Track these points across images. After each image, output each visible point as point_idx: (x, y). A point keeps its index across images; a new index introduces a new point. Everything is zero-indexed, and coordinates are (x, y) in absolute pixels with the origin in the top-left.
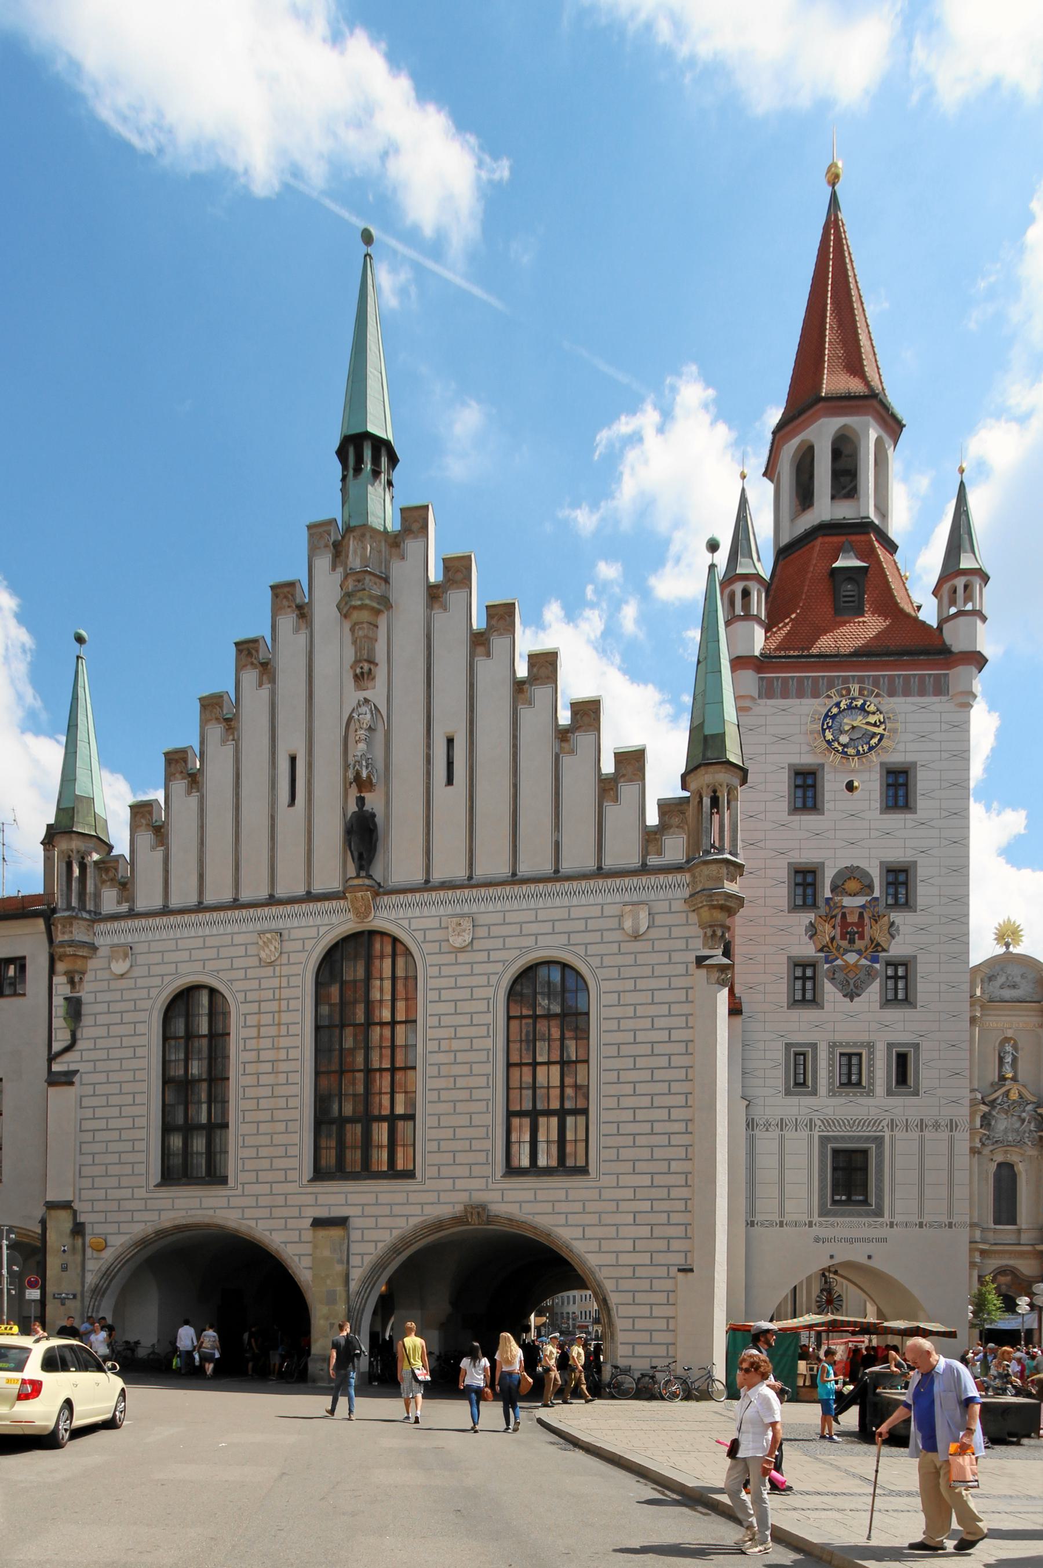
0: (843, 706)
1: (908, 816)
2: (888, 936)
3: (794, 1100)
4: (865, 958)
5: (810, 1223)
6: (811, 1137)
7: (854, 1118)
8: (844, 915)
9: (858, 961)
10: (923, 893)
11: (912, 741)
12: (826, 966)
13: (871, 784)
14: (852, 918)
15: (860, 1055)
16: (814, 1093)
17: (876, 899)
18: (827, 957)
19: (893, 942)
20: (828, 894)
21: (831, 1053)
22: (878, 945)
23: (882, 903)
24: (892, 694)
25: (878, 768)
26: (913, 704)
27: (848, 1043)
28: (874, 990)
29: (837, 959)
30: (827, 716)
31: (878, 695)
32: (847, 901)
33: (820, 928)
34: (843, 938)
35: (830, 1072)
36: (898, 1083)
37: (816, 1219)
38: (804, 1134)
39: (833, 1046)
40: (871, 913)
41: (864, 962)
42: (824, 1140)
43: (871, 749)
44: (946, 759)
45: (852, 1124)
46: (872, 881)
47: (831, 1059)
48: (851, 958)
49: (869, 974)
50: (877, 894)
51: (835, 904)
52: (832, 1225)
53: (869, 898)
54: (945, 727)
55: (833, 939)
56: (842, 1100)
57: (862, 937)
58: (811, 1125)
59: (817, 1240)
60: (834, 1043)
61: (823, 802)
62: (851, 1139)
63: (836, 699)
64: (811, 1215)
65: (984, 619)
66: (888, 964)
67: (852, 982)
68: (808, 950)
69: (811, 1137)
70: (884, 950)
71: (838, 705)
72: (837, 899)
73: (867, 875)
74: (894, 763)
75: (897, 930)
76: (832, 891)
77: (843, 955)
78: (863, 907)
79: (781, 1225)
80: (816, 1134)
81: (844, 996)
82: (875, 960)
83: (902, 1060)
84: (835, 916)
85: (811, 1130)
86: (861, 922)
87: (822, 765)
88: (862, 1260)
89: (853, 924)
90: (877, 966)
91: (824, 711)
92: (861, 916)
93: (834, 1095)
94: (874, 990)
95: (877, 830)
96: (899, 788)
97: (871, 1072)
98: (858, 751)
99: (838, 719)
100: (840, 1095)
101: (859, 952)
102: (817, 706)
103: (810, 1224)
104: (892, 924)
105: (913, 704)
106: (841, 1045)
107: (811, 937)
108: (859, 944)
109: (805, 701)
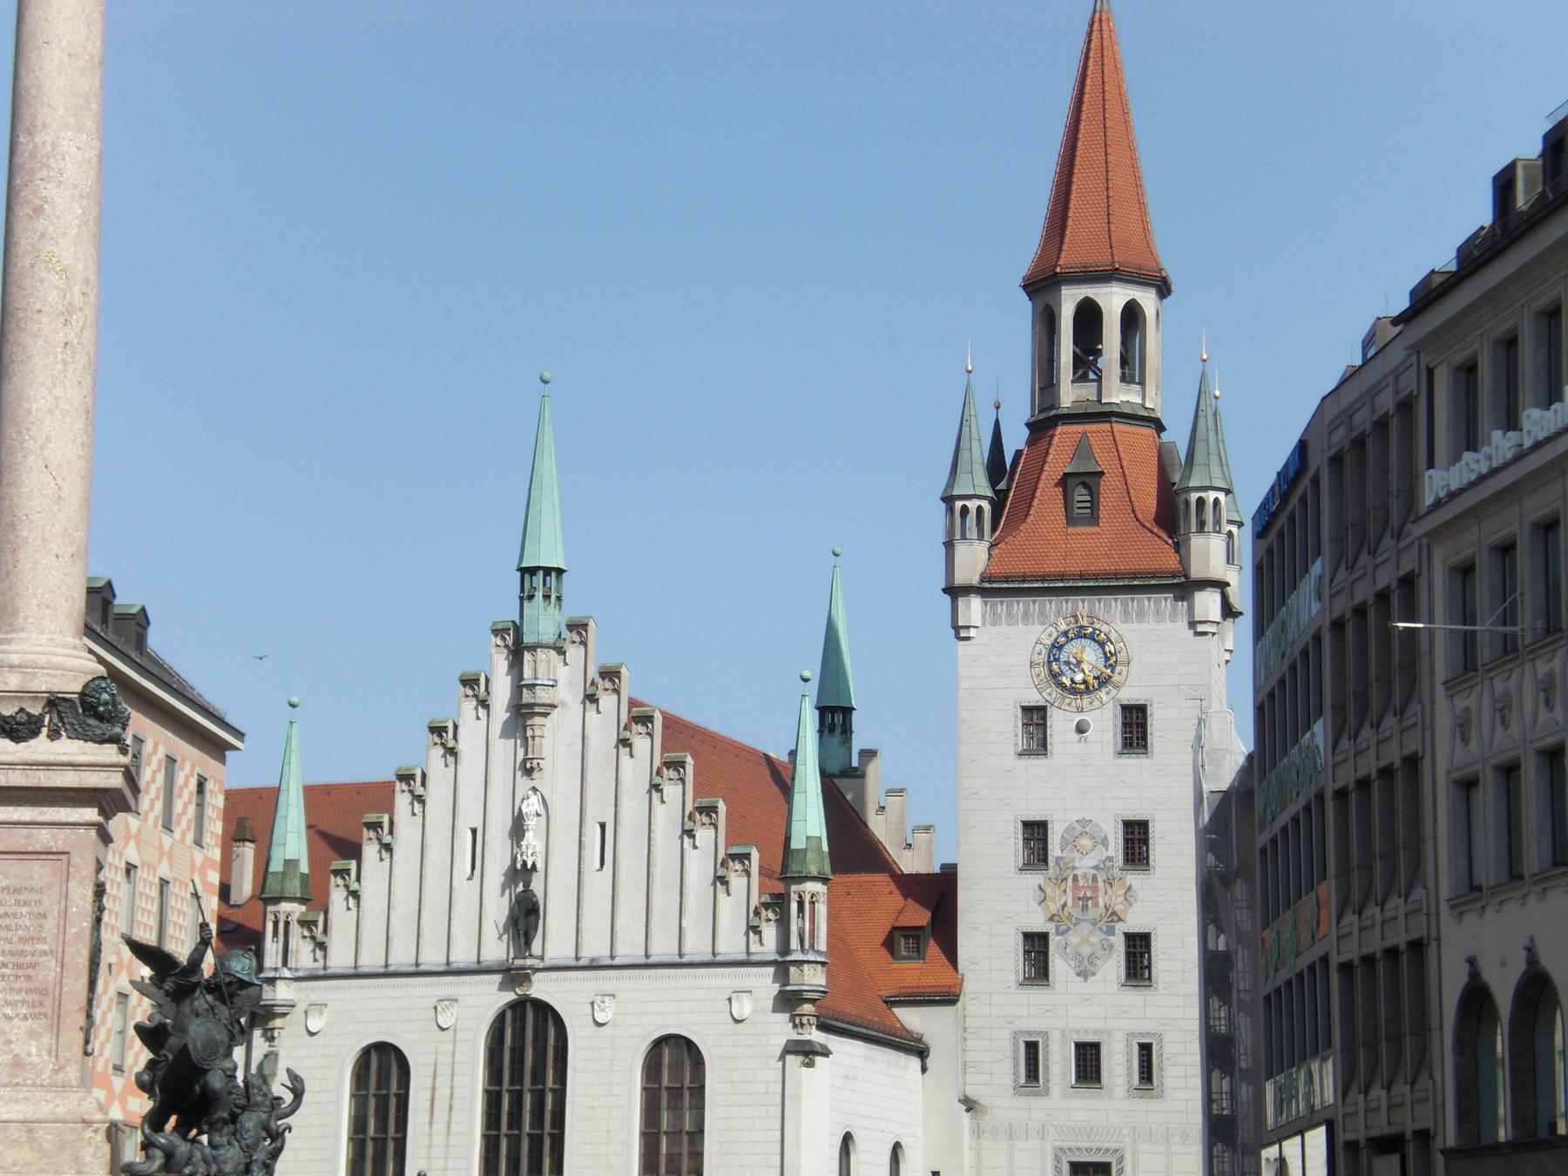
3: (1023, 1101)
8: (1075, 878)
13: (1105, 722)
16: (1047, 1092)
17: (1110, 859)
22: (1114, 913)
30: (1053, 646)
34: (1075, 905)
36: (1142, 1079)
55: (1065, 905)
57: (1096, 905)
62: (1089, 1150)
63: (1063, 627)
68: (1038, 924)
70: (1120, 920)
71: (1065, 633)
78: (1096, 868)
81: (1078, 974)
82: (1111, 931)
83: (1146, 1049)
84: (1065, 879)
86: (1095, 889)
91: (1049, 642)
92: (1094, 879)
96: (1135, 727)
104: (1130, 888)
108: (1093, 913)
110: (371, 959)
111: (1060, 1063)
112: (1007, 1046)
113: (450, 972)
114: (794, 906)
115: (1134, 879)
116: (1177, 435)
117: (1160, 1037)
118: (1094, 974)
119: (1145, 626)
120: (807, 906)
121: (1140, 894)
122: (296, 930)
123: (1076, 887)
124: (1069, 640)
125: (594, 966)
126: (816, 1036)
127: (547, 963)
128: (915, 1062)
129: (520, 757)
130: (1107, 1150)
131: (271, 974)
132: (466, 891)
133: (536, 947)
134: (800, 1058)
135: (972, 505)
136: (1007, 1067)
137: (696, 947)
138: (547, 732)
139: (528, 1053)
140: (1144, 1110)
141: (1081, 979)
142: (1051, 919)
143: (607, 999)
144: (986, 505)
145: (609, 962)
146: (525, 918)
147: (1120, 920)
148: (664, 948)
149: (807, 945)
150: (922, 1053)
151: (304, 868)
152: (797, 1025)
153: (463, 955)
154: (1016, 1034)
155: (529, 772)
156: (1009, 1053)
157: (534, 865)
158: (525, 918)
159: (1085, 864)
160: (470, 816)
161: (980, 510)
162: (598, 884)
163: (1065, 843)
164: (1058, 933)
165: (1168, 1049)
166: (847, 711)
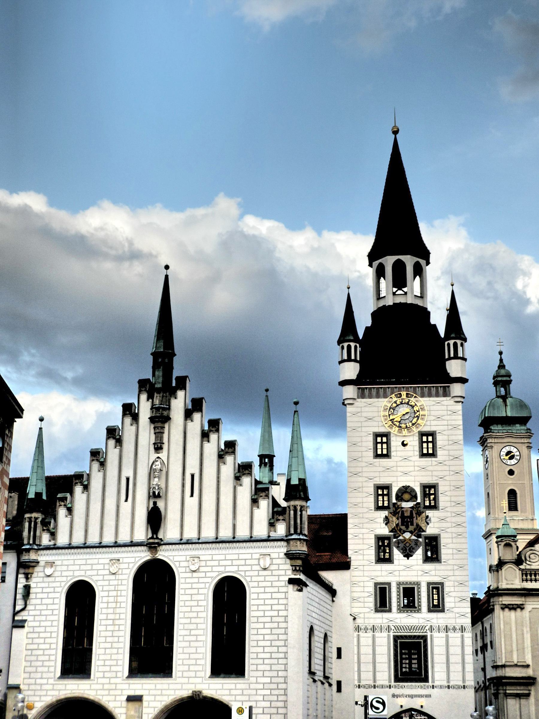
0: (398, 403)
1: (433, 459)
2: (425, 523)
3: (379, 615)
4: (415, 535)
5: (390, 686)
6: (389, 636)
7: (411, 625)
9: (411, 536)
10: (443, 500)
11: (434, 420)
12: (394, 540)
14: (407, 514)
15: (413, 589)
16: (390, 611)
17: (419, 504)
18: (394, 535)
19: (428, 526)
20: (394, 501)
21: (398, 588)
22: (421, 528)
23: (422, 506)
24: (423, 396)
25: (417, 434)
26: (433, 401)
27: (407, 583)
28: (419, 553)
29: (400, 536)
30: (390, 408)
31: (415, 397)
32: (405, 505)
33: (391, 519)
35: (398, 599)
37: (393, 683)
38: (385, 634)
39: (399, 584)
40: (418, 510)
41: (414, 537)
42: (396, 638)
43: (413, 424)
44: (451, 429)
45: (410, 628)
46: (416, 494)
47: (399, 592)
48: (407, 535)
49: (416, 544)
50: (419, 500)
51: (398, 506)
52: (402, 687)
53: (415, 503)
54: (449, 413)
55: (397, 525)
56: (404, 615)
57: (412, 524)
58: (389, 629)
59: (394, 696)
60: (400, 583)
61: (390, 452)
62: (410, 637)
64: (390, 682)
65: (465, 360)
66: (426, 538)
67: (408, 548)
69: (389, 636)
70: (424, 531)
71: (395, 402)
72: (399, 503)
73: (413, 490)
74: (425, 431)
75: (430, 520)
76: (396, 499)
77: (403, 534)
79: (375, 688)
80: (392, 634)
81: (404, 556)
82: (419, 536)
85: (389, 632)
86: (411, 516)
87: (390, 433)
88: (419, 708)
89: (407, 517)
90: (420, 540)
91: (389, 405)
93: (400, 612)
94: (419, 553)
95: (418, 466)
97: (419, 599)
98: (407, 426)
99: (397, 409)
100: (404, 612)
101: (411, 532)
102: (384, 402)
103: (390, 687)
104: (427, 517)
105: (433, 401)
106: (403, 583)
107: (386, 524)
108: (411, 528)
109: (380, 400)
110: (78, 539)
111: (395, 597)
112: (372, 590)
113: (116, 545)
114: (292, 512)
115: (429, 513)
116: (439, 320)
117: (442, 584)
118: (412, 556)
119: (432, 399)
120: (299, 513)
121: (433, 520)
122: (39, 525)
123: (403, 517)
124: (397, 405)
125: (189, 542)
126: (302, 577)
127: (165, 542)
128: (328, 597)
129: (153, 440)
130: (419, 637)
131: (28, 547)
132: (126, 507)
133: (160, 536)
134: (296, 587)
135: (353, 345)
136: (372, 599)
137: (243, 532)
138: (166, 430)
139: (154, 588)
140: (437, 619)
141: (406, 558)
142: (390, 532)
143: (196, 560)
144: (358, 345)
145: (197, 541)
146: (155, 519)
147: (424, 531)
148: (225, 533)
149: (299, 531)
150: (333, 592)
151: (44, 497)
152: (295, 570)
153: (124, 538)
154: (376, 584)
155: (158, 448)
156: (373, 593)
157: (159, 493)
158: (155, 519)
159: (407, 505)
160: (127, 472)
161: (356, 347)
162: (191, 503)
163: (398, 497)
164: (395, 537)
165: (446, 590)
166: (271, 457)
